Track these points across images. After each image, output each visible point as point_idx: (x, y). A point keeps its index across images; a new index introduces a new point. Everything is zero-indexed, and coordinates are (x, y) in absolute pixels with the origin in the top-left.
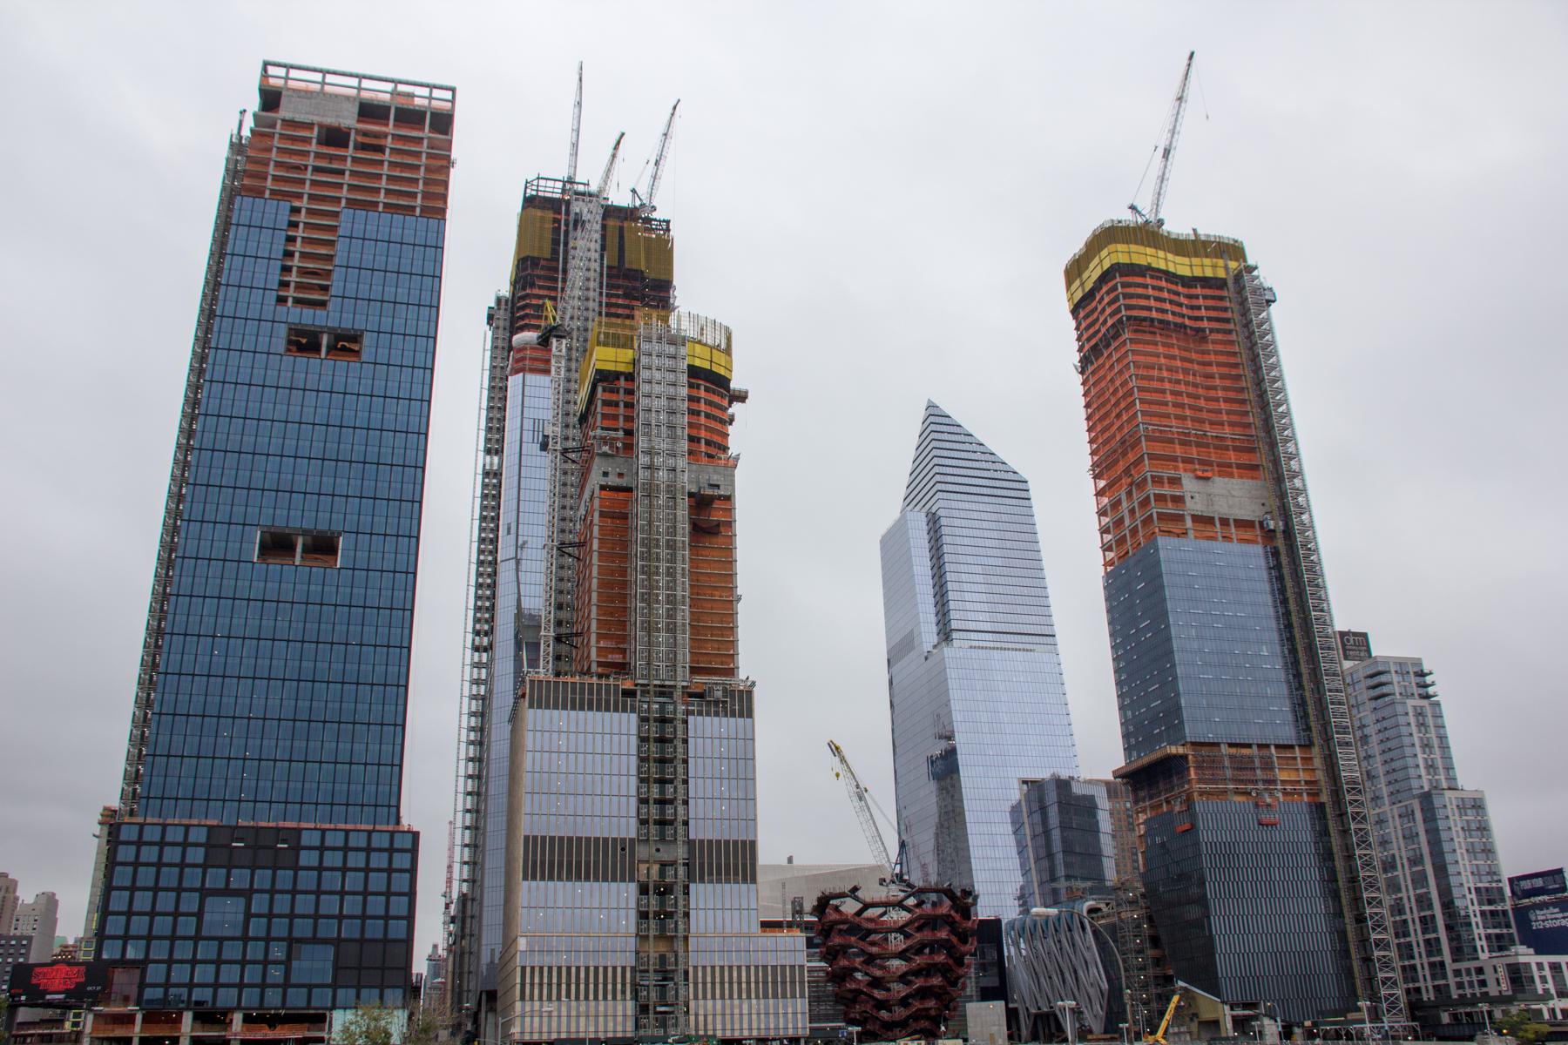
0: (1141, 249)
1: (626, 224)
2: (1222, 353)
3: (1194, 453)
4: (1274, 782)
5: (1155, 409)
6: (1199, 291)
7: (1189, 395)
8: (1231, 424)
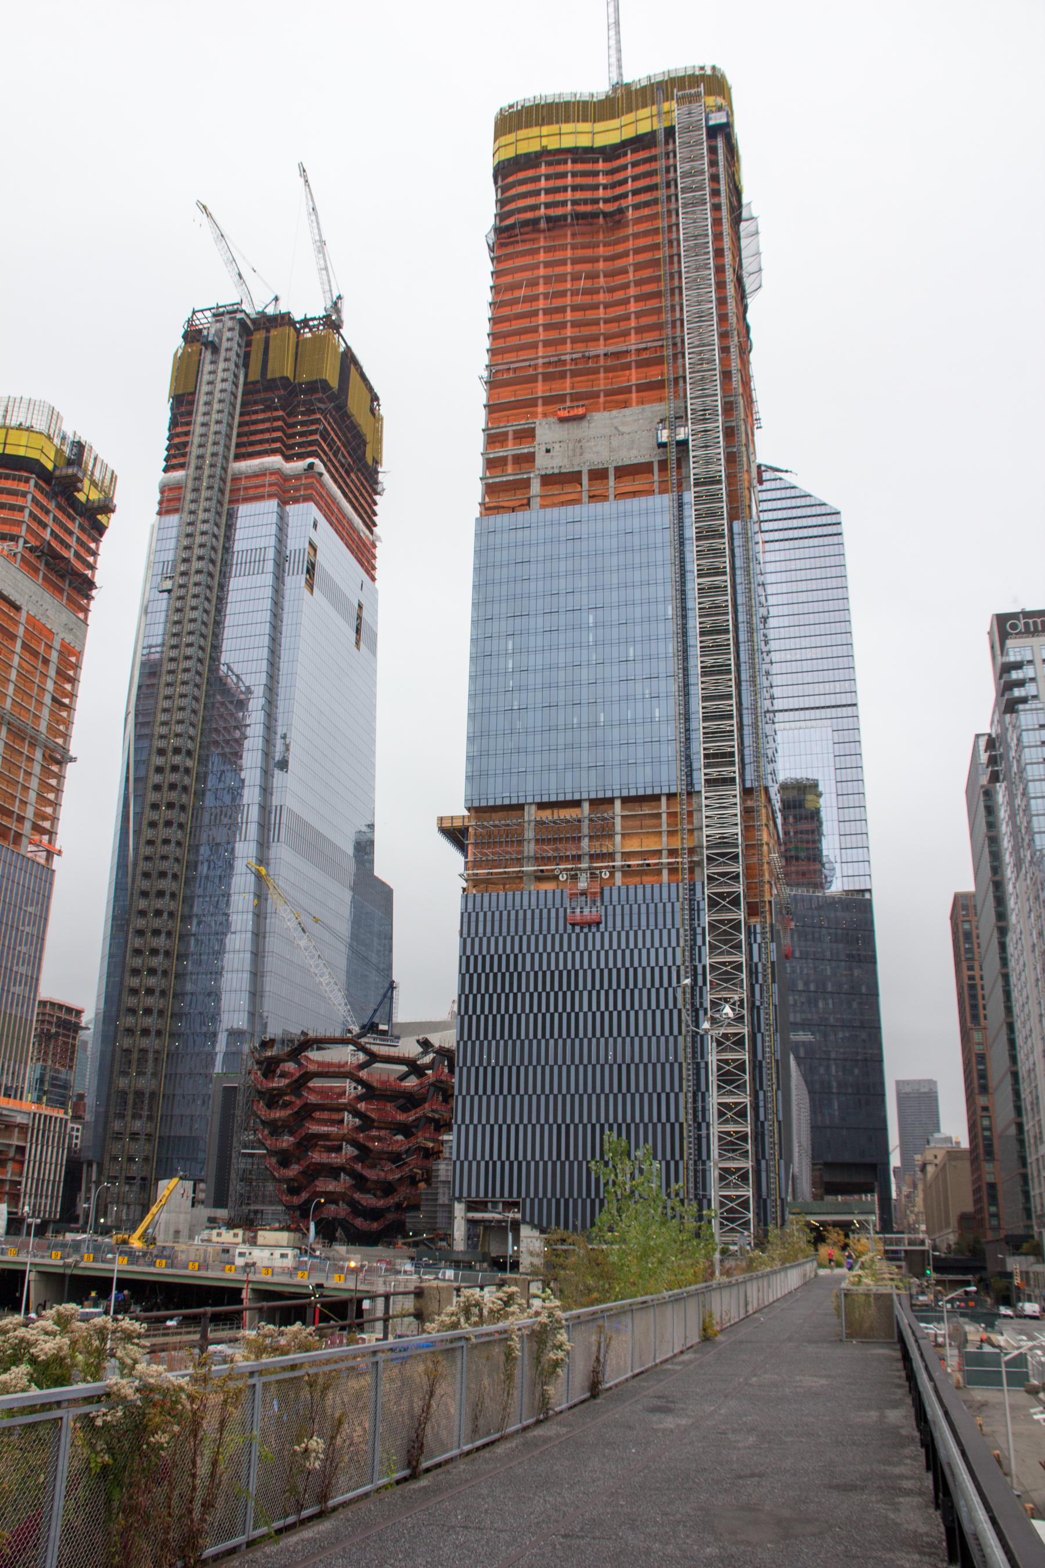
0: (535, 131)
1: (273, 333)
2: (646, 234)
3: (567, 386)
4: (611, 856)
5: (514, 341)
6: (630, 158)
7: (575, 308)
8: (639, 330)
